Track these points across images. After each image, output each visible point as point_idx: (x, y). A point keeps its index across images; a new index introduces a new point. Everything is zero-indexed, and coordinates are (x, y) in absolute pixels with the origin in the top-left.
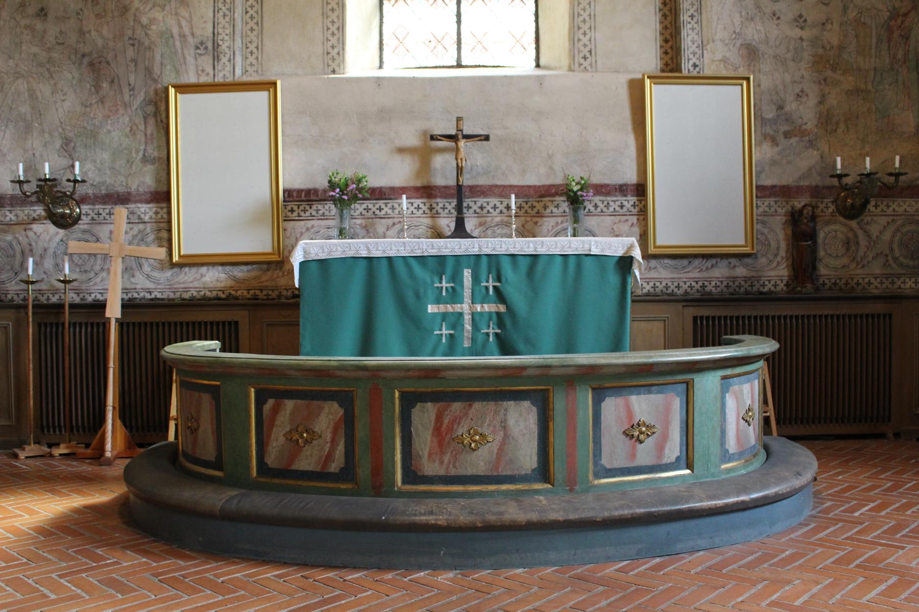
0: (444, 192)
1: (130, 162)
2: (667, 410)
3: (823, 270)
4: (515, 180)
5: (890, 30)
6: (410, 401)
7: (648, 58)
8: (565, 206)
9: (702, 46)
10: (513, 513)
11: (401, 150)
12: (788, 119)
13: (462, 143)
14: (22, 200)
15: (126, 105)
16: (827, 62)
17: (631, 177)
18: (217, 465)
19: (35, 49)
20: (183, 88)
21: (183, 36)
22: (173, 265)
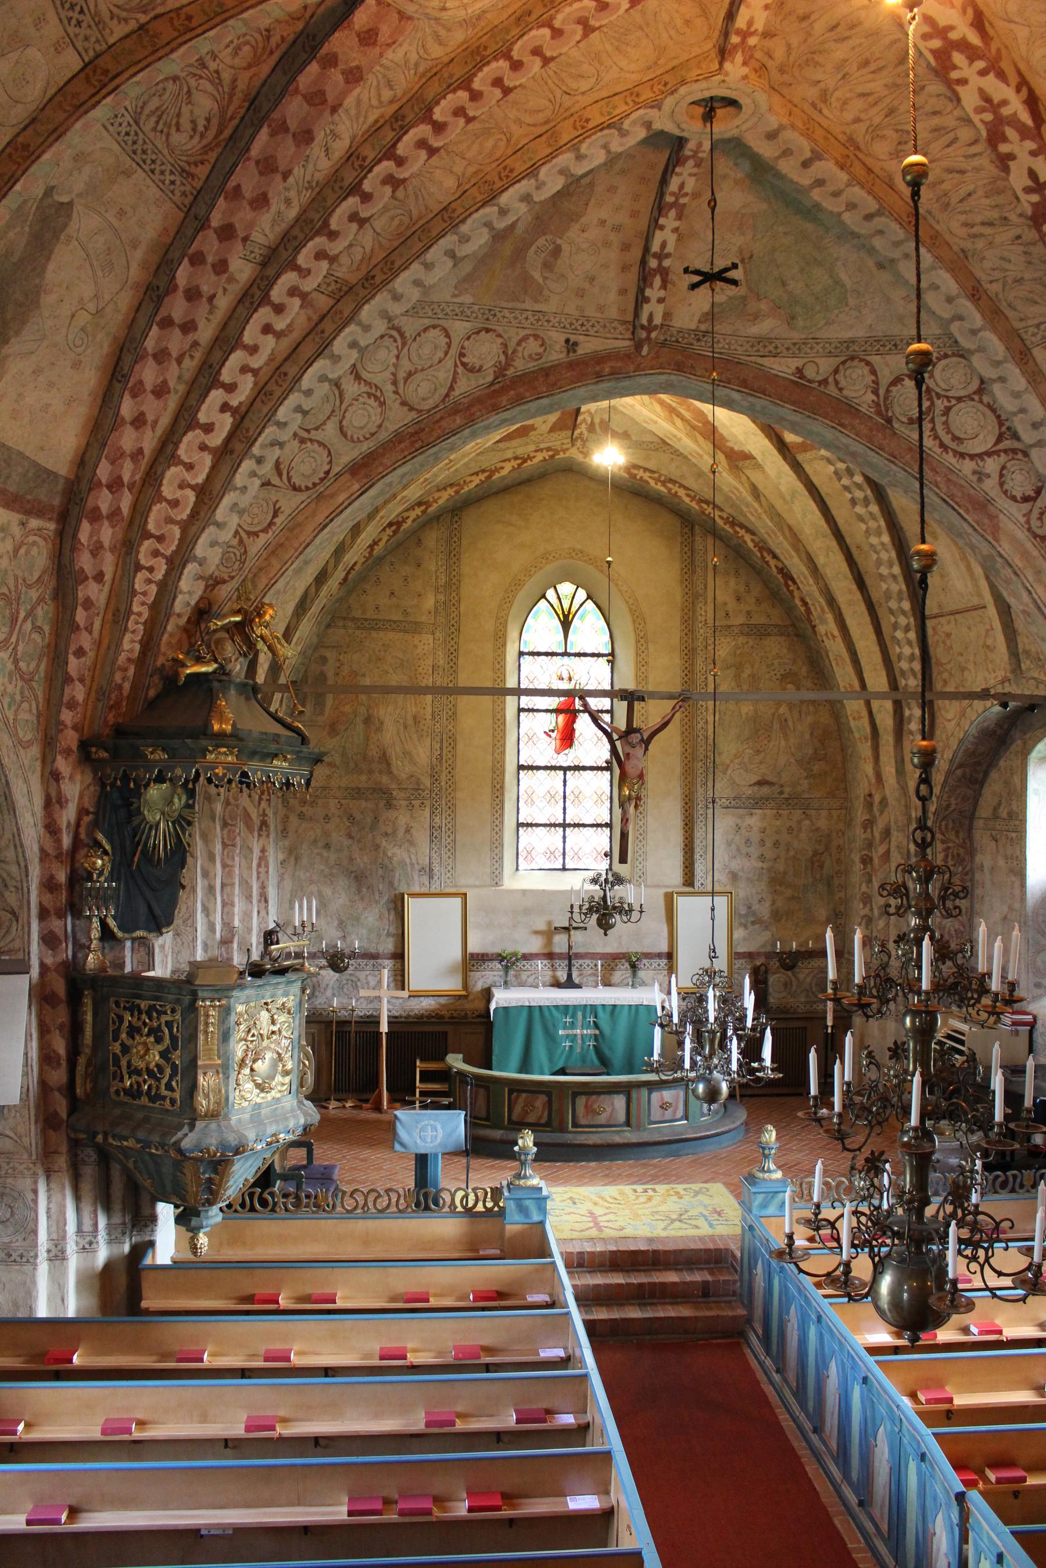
0: (560, 956)
1: (379, 936)
2: (678, 1096)
3: (771, 1000)
5: (813, 863)
6: (575, 1095)
7: (674, 876)
8: (627, 965)
10: (617, 1139)
11: (536, 932)
12: (754, 914)
13: (572, 932)
15: (377, 902)
16: (776, 881)
17: (664, 948)
18: (487, 1119)
19: (322, 867)
21: (412, 864)
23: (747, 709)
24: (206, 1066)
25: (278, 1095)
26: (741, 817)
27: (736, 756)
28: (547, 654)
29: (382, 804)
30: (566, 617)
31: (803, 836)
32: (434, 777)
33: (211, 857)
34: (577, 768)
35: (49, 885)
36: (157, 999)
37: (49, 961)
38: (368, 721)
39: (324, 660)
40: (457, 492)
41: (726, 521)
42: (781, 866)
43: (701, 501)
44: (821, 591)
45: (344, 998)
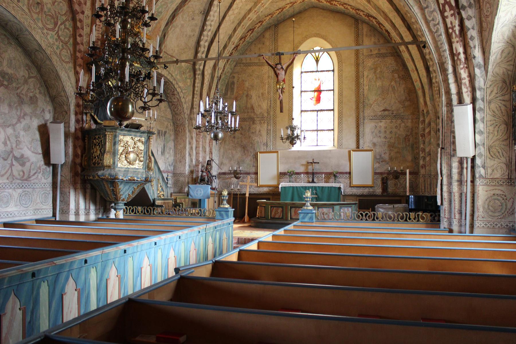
4: (324, 171)
7: (354, 146)
9: (364, 143)
11: (302, 165)
12: (382, 158)
14: (230, 173)
15: (250, 155)
16: (391, 146)
17: (348, 170)
20: (260, 153)
22: (258, 187)
23: (379, 83)
24: (108, 152)
25: (137, 167)
26: (377, 123)
27: (375, 101)
28: (311, 72)
29: (251, 123)
30: (317, 58)
31: (401, 129)
32: (268, 113)
33: (192, 138)
34: (321, 110)
35: (77, 105)
36: (100, 134)
37: (77, 127)
38: (247, 96)
39: (234, 77)
40: (272, 17)
41: (366, 15)
42: (392, 141)
43: (356, 9)
44: (397, 34)
45: (236, 186)
